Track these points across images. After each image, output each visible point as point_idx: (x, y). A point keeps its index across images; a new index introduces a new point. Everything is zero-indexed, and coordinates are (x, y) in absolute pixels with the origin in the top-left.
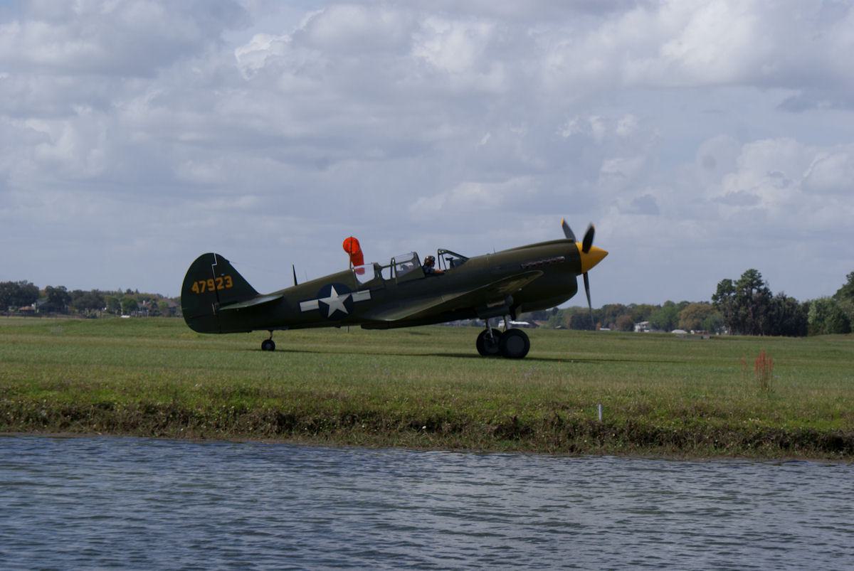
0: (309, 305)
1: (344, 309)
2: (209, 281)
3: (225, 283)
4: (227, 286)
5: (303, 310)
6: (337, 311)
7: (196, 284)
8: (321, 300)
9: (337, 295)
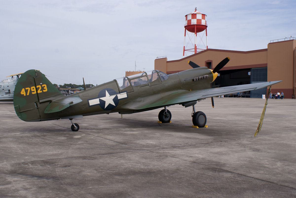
0: (94, 102)
1: (114, 104)
2: (32, 88)
3: (43, 88)
4: (44, 91)
5: (91, 105)
6: (110, 105)
7: (23, 90)
8: (100, 98)
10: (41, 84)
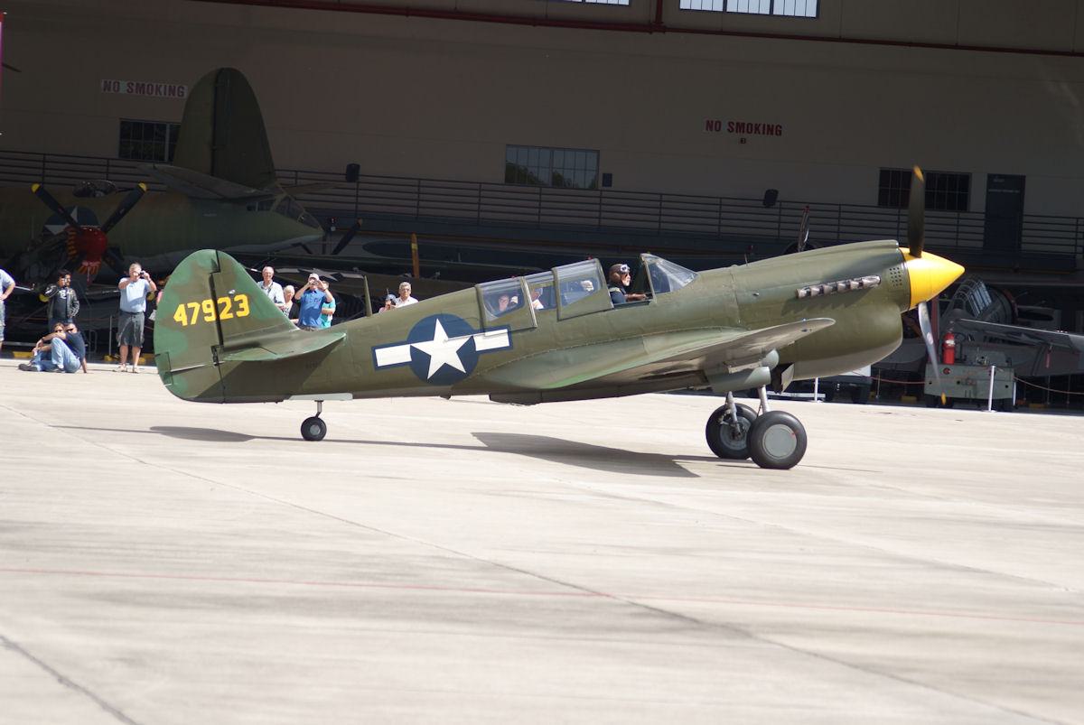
1: (459, 366)
2: (205, 303)
3: (236, 307)
4: (240, 314)
5: (380, 364)
6: (446, 368)
7: (181, 308)
8: (413, 345)
9: (447, 338)
10: (231, 292)
